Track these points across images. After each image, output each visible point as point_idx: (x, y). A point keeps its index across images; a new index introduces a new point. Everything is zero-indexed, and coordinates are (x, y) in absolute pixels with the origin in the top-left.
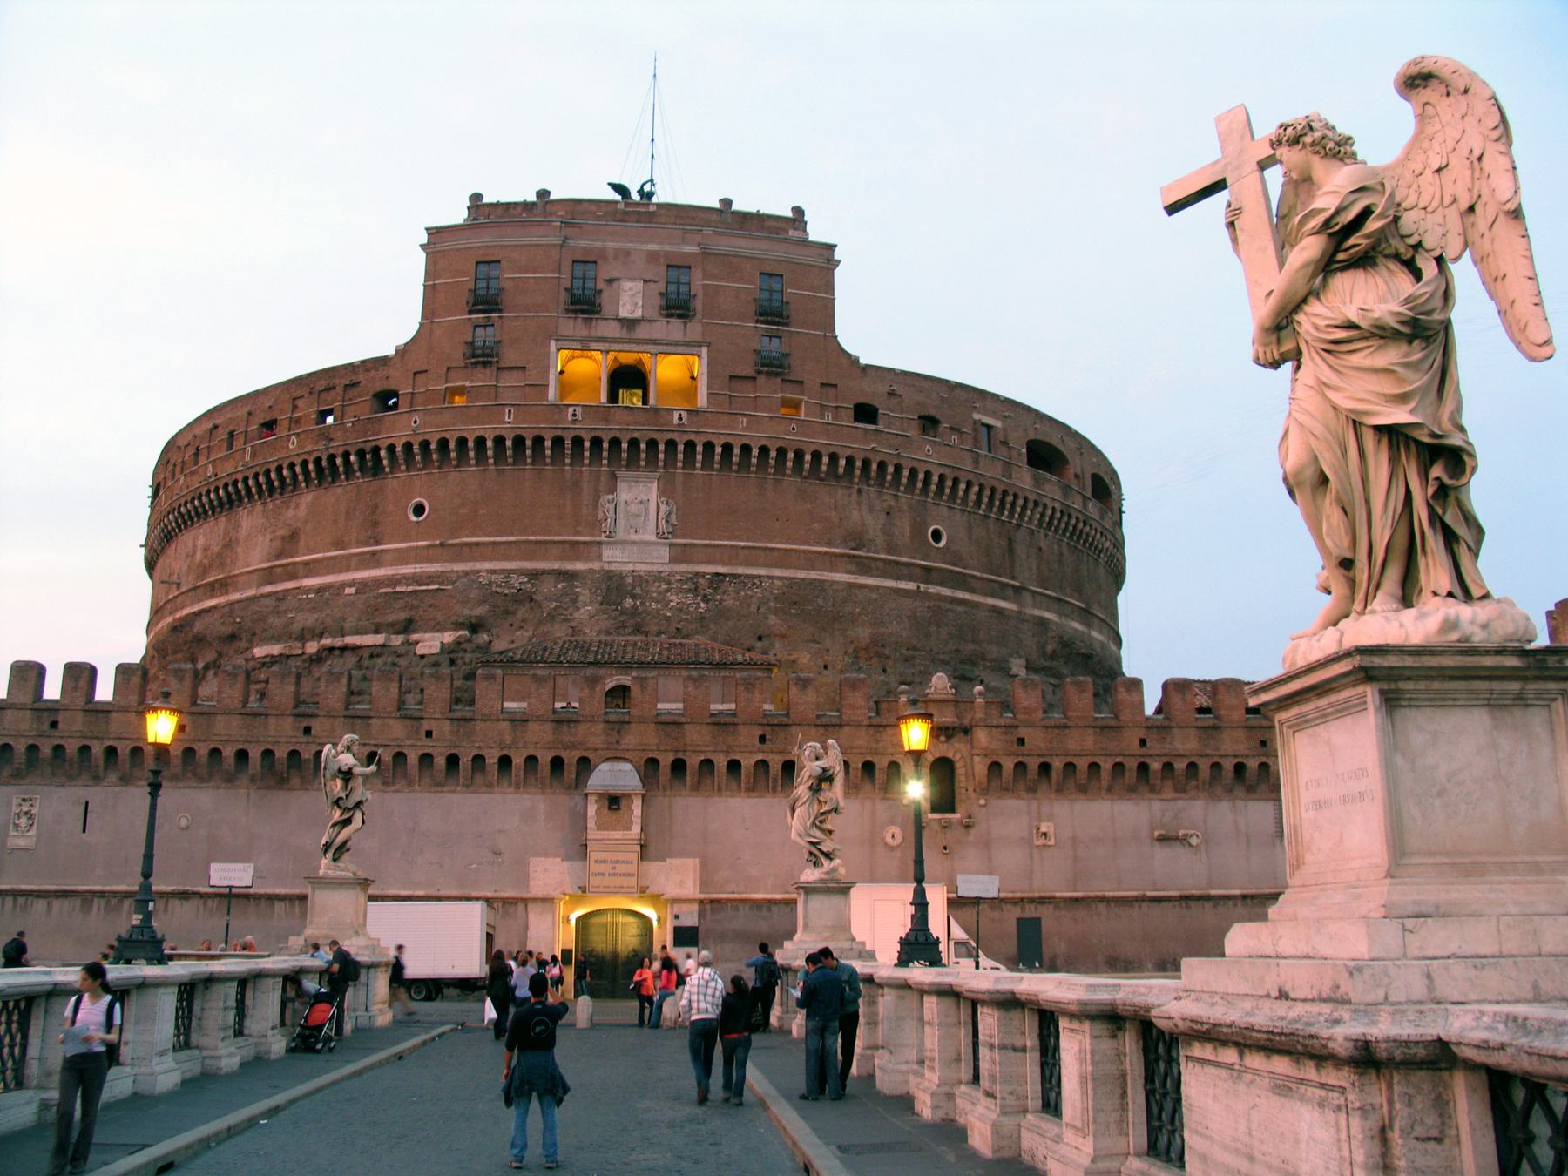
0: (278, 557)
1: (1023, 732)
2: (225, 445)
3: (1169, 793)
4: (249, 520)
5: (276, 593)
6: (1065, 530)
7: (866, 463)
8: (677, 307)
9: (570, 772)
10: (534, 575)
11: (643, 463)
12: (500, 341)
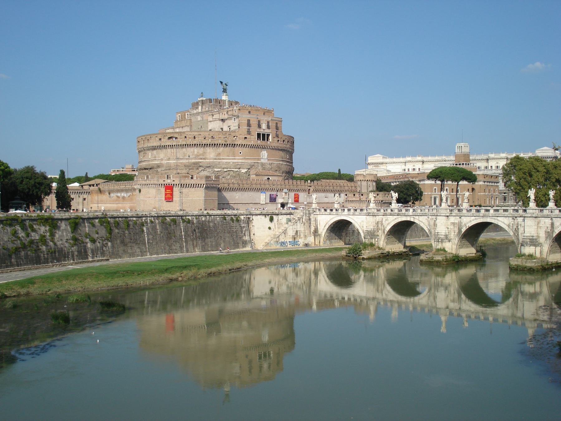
4: (209, 150)
8: (268, 127)
10: (255, 163)
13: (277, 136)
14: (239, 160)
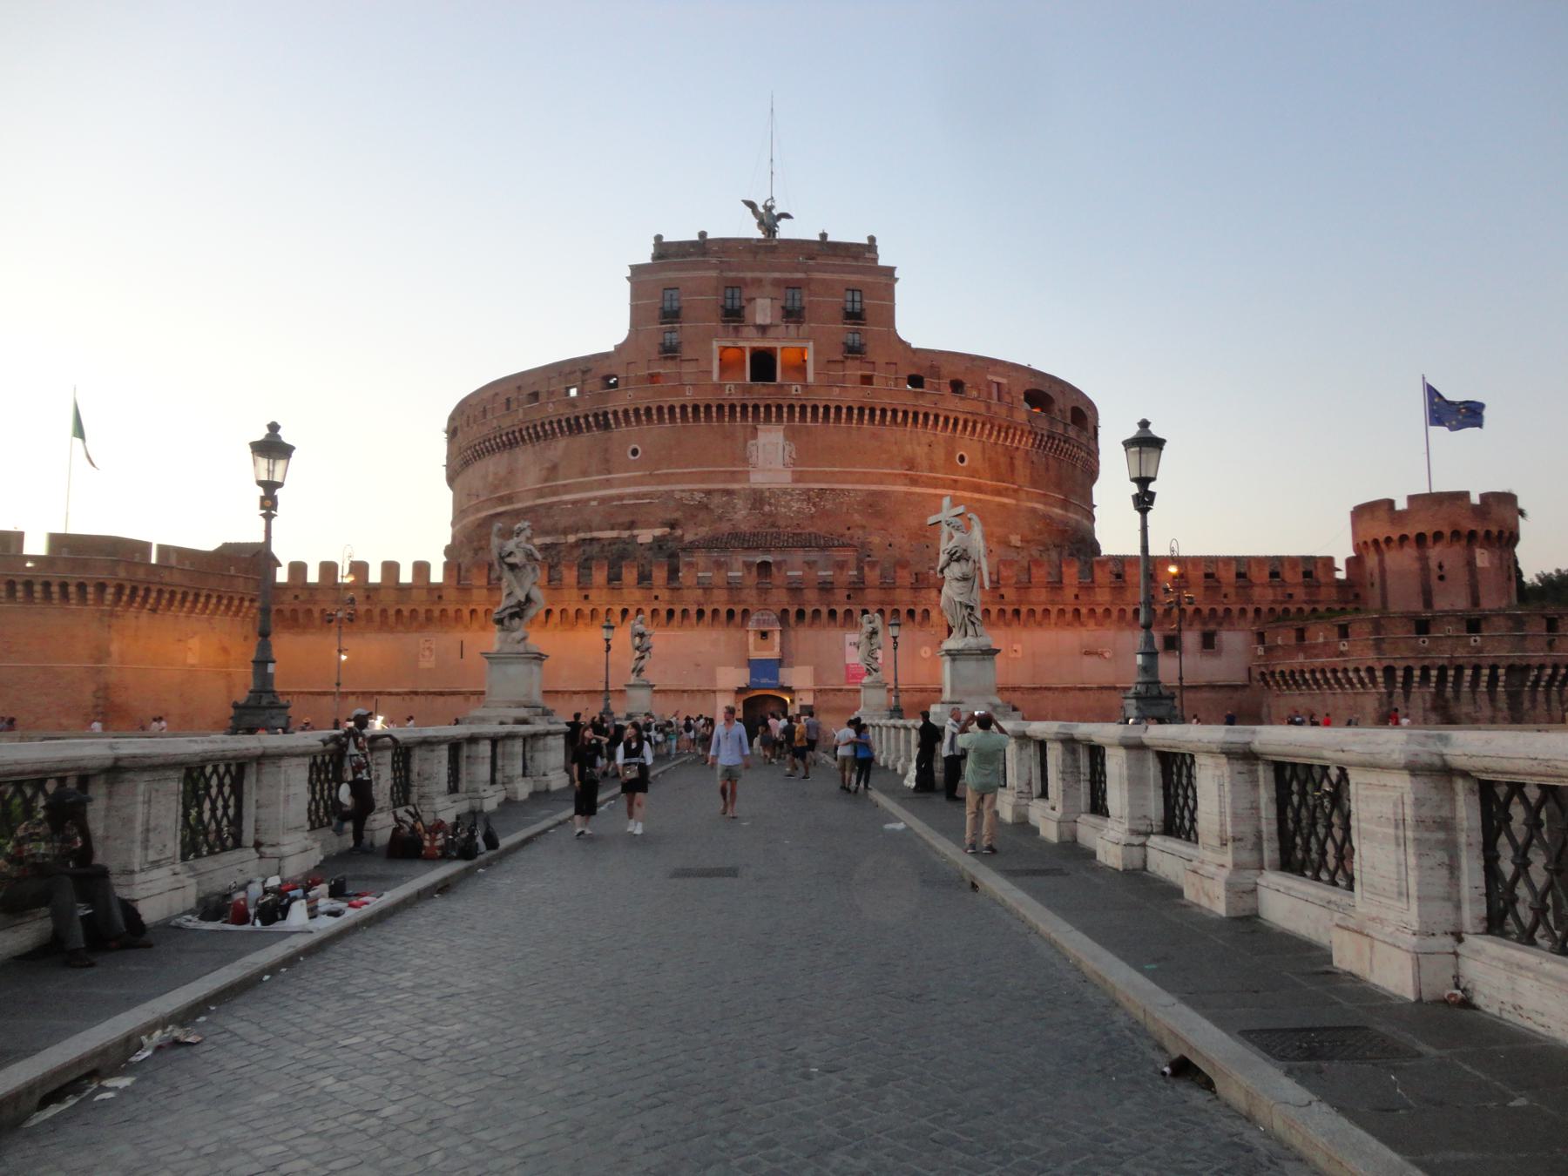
0: (546, 480)
1: (1003, 591)
2: (504, 408)
3: (1091, 624)
5: (545, 504)
6: (1050, 448)
7: (916, 414)
8: (792, 315)
9: (738, 618)
10: (709, 493)
11: (774, 420)
12: (680, 343)
13: (854, 351)
14: (626, 485)
